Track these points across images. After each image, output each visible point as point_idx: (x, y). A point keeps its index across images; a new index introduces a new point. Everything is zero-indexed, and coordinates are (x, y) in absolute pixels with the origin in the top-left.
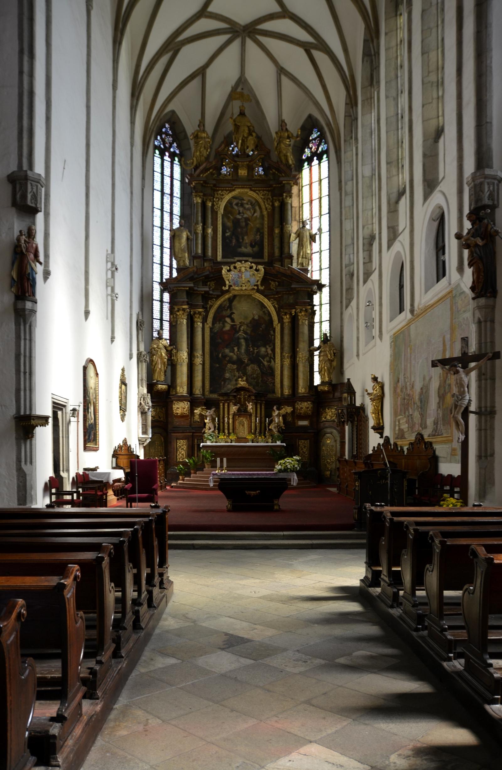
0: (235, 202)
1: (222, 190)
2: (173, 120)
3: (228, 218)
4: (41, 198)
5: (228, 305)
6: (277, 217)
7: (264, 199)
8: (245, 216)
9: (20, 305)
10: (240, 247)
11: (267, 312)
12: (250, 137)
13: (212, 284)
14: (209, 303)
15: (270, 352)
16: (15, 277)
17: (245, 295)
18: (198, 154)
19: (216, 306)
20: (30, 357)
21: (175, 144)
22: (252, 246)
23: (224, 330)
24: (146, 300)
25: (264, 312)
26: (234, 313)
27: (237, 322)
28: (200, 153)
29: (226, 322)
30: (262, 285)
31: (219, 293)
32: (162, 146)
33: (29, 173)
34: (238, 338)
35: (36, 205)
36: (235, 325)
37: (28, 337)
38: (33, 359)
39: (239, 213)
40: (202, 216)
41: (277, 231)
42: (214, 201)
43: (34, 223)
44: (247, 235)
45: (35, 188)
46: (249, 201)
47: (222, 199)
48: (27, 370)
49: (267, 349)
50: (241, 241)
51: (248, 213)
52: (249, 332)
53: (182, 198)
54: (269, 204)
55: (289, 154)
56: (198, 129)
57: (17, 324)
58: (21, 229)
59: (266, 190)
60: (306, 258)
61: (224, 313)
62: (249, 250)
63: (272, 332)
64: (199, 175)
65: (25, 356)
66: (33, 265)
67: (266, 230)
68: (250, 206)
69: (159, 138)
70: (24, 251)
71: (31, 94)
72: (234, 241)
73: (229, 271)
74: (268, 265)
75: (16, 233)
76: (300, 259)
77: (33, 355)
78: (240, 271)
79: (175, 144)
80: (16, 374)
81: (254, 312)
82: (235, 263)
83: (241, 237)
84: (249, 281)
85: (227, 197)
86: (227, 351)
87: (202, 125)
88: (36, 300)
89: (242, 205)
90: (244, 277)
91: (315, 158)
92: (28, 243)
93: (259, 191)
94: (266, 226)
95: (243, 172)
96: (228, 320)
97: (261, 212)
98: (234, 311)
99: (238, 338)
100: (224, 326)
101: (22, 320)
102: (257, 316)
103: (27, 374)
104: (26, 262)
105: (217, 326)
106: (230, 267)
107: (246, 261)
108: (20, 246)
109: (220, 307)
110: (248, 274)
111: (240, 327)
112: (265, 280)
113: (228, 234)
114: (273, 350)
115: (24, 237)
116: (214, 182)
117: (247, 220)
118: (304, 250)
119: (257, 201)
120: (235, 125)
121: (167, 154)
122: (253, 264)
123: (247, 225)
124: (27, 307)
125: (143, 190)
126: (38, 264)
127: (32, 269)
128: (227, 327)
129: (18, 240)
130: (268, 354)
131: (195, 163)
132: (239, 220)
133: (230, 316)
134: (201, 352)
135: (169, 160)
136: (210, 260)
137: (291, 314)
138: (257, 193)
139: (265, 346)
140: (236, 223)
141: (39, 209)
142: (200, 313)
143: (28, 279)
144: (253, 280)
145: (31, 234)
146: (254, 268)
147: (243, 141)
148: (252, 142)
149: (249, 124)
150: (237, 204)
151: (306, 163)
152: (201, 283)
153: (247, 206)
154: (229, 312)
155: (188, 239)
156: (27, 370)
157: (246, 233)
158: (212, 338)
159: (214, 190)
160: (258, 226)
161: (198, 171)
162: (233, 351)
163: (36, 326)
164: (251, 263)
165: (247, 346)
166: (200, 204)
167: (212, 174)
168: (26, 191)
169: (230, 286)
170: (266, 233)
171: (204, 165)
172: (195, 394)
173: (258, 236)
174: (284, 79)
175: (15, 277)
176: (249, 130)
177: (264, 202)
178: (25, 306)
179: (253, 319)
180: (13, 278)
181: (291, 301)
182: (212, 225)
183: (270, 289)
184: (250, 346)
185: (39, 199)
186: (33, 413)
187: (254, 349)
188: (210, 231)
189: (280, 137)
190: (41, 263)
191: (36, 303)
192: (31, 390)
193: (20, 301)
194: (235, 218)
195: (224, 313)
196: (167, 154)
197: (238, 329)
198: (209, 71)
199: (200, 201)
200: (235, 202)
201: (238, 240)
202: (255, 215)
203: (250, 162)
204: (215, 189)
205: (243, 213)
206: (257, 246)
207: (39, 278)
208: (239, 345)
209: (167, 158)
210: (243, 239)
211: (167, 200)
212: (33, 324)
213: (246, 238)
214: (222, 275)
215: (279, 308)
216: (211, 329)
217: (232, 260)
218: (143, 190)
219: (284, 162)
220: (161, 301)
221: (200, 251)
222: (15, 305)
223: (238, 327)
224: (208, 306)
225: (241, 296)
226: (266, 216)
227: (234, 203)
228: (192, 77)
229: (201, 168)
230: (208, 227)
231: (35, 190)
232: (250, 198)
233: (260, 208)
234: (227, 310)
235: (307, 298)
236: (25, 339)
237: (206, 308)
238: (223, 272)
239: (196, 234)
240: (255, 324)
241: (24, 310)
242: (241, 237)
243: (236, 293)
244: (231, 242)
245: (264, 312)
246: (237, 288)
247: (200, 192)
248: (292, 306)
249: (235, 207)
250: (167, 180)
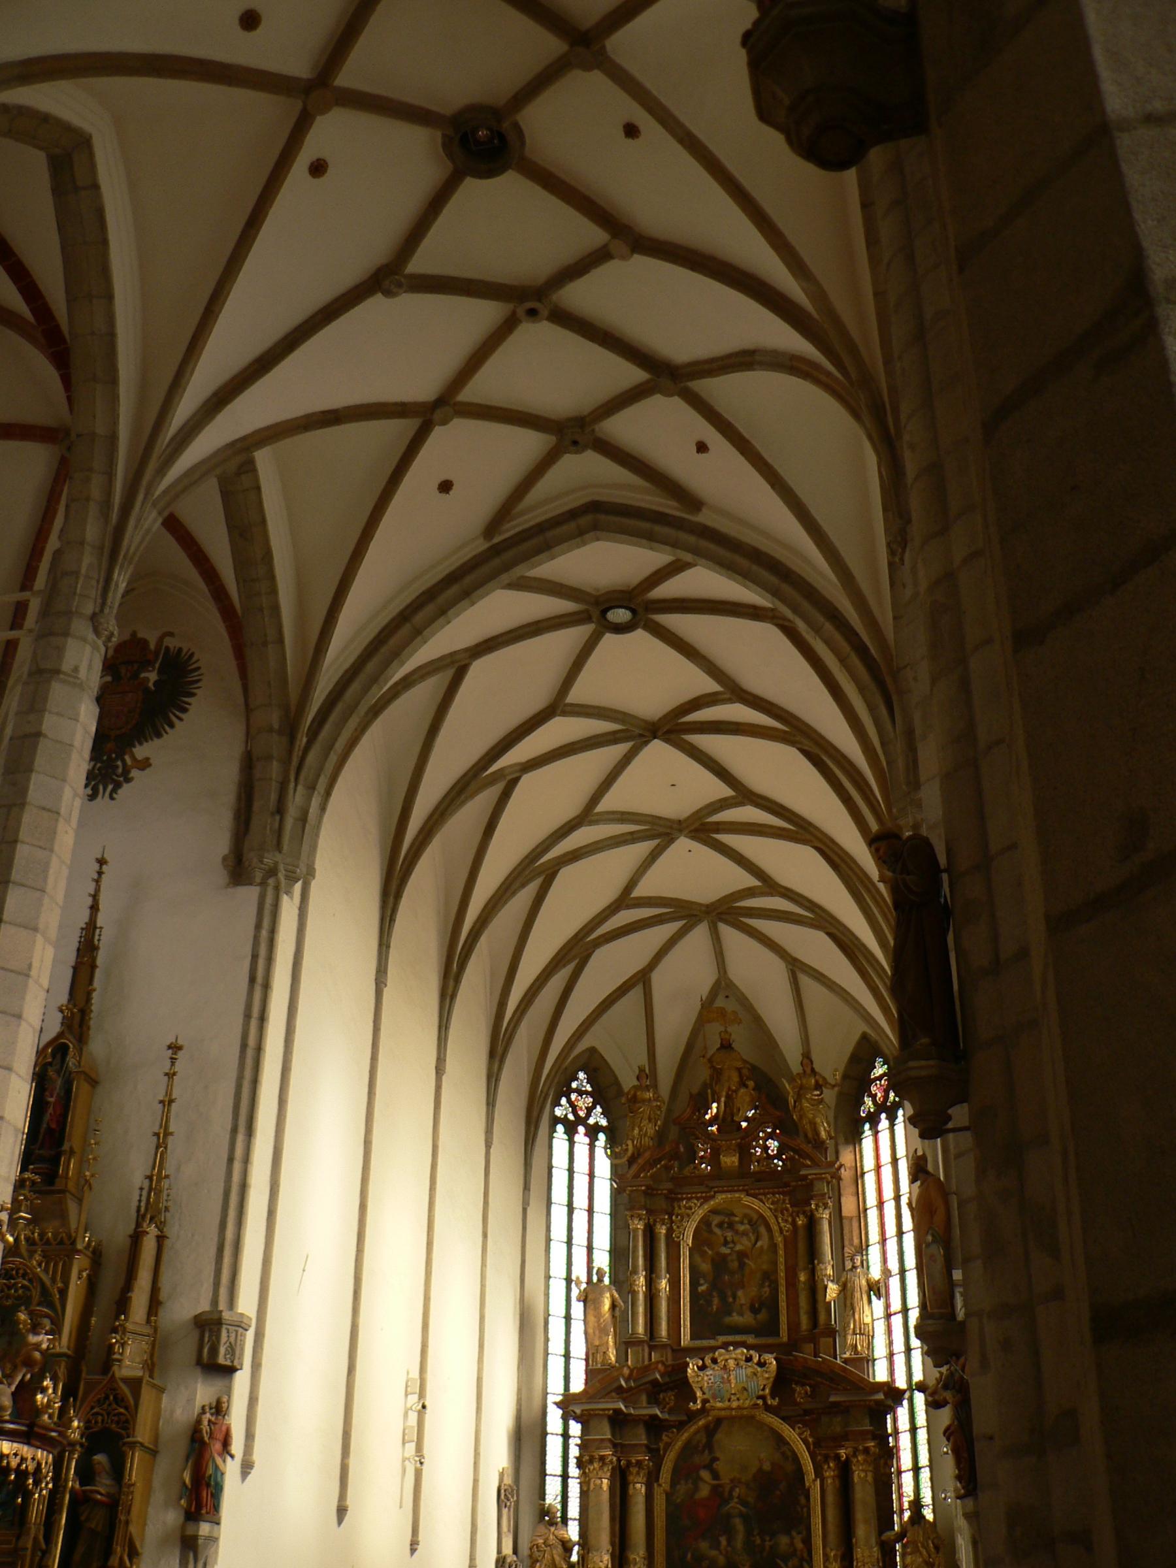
0: (716, 1220)
1: (689, 1199)
2: (594, 1065)
3: (703, 1254)
5: (704, 1441)
6: (802, 1246)
7: (776, 1210)
8: (738, 1247)
10: (729, 1314)
11: (789, 1454)
12: (743, 1090)
13: (670, 1397)
14: (664, 1437)
15: (799, 1545)
17: (741, 1417)
18: (636, 1131)
19: (679, 1444)
21: (599, 1109)
22: (754, 1310)
23: (697, 1496)
24: (527, 1438)
25: (783, 1454)
26: (716, 1459)
27: (725, 1480)
28: (641, 1130)
29: (702, 1479)
30: (773, 1398)
31: (685, 1418)
32: (571, 1117)
34: (729, 1516)
36: (719, 1486)
39: (726, 1243)
40: (645, 1256)
41: (802, 1277)
42: (672, 1222)
44: (743, 1287)
46: (745, 1216)
47: (689, 1216)
49: (792, 1538)
50: (731, 1300)
51: (745, 1240)
52: (751, 1500)
53: (614, 1215)
54: (786, 1221)
55: (818, 1120)
56: (636, 1083)
59: (779, 1193)
60: (860, 1334)
61: (697, 1459)
62: (747, 1319)
63: (803, 1501)
64: (636, 1176)
67: (782, 1274)
68: (748, 1227)
69: (564, 1101)
72: (716, 1301)
73: (702, 1368)
74: (784, 1352)
76: (849, 1337)
78: (725, 1367)
79: (599, 1109)
81: (762, 1455)
82: (713, 1349)
83: (729, 1293)
84: (745, 1389)
85: (700, 1213)
86: (704, 1545)
89: (731, 1226)
90: (733, 1381)
91: (883, 1116)
93: (765, 1194)
94: (782, 1267)
95: (730, 1160)
96: (705, 1474)
97: (771, 1237)
98: (718, 1455)
99: (729, 1516)
100: (696, 1489)
102: (768, 1464)
105: (683, 1488)
106: (703, 1360)
107: (737, 1345)
109: (687, 1445)
110: (743, 1373)
111: (732, 1490)
112: (782, 1383)
113: (702, 1288)
114: (807, 1542)
116: (670, 1185)
117: (742, 1255)
118: (857, 1317)
119: (761, 1216)
120: (713, 1067)
121: (581, 1129)
122: (752, 1352)
123: (742, 1265)
125: (525, 1211)
128: (704, 1492)
130: (795, 1550)
131: (630, 1153)
132: (725, 1256)
133: (709, 1467)
134: (642, 1551)
135: (587, 1140)
136: (664, 1346)
137: (838, 1457)
138: (761, 1200)
139: (788, 1533)
140: (720, 1263)
142: (639, 1464)
144: (755, 1386)
146: (756, 1359)
147: (728, 1097)
148: (747, 1099)
149: (739, 1064)
150: (720, 1225)
151: (867, 1126)
152: (644, 1398)
153: (741, 1228)
154: (706, 1457)
155: (613, 1306)
157: (742, 1285)
159: (673, 1200)
160: (765, 1267)
161: (635, 1168)
162: (716, 1545)
164: (749, 1347)
165: (749, 1533)
166: (640, 1233)
167: (668, 1168)
169: (705, 1401)
170: (782, 1282)
171: (647, 1155)
173: (767, 1289)
174: (804, 980)
176: (741, 1076)
177: (776, 1218)
179: (760, 1470)
181: (838, 1429)
182: (668, 1271)
183: (796, 1404)
184: (756, 1532)
187: (763, 1541)
188: (664, 1284)
189: (801, 1087)
194: (718, 1254)
195: (697, 1459)
196: (581, 1129)
197: (726, 1494)
199: (640, 1226)
200: (716, 1220)
201: (723, 1299)
202: (759, 1244)
203: (742, 1139)
204: (672, 1198)
205: (733, 1242)
206: (764, 1310)
208: (730, 1532)
209: (581, 1137)
210: (735, 1297)
211: (580, 1218)
213: (740, 1293)
215: (814, 1443)
216: (668, 1495)
217: (712, 1343)
218: (525, 1211)
219: (810, 1135)
220: (566, 1436)
221: (641, 1329)
223: (727, 1489)
224: (661, 1445)
225: (732, 1418)
226: (781, 1246)
227: (715, 1223)
228: (622, 991)
229: (641, 1161)
230: (659, 1277)
232: (747, 1211)
233: (769, 1230)
234: (703, 1451)
235: (867, 1421)
237: (658, 1450)
238: (691, 1370)
239: (634, 1293)
240: (764, 1482)
242: (729, 1293)
243: (723, 1413)
244: (709, 1303)
245: (783, 1454)
246: (719, 1405)
247: (639, 1209)
248: (839, 1440)
249: (717, 1231)
250: (581, 1182)
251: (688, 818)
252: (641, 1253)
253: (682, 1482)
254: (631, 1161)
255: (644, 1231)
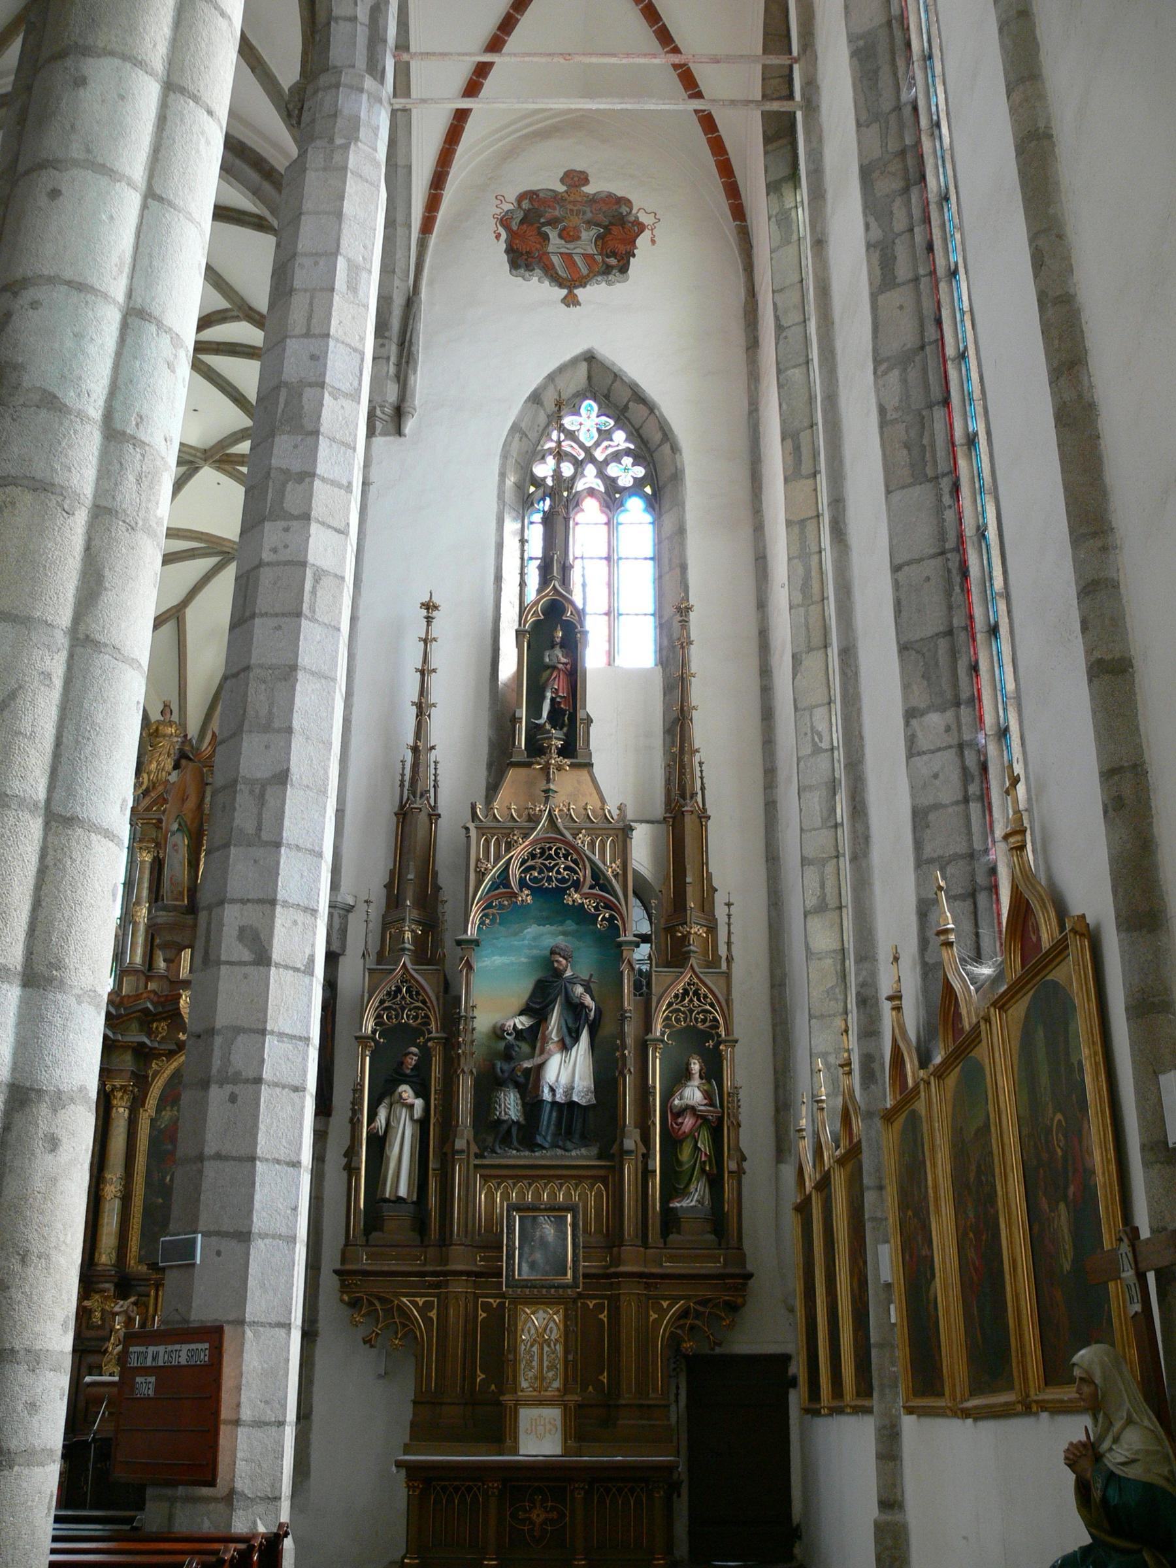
13: (162, 1027)
19: (168, 1073)
31: (174, 1047)
40: (150, 888)
64: (148, 809)
87: (168, 710)
105: (167, 1114)
131: (144, 787)
136: (161, 977)
158: (154, 1142)
166: (148, 866)
172: (97, 1265)
198: (190, 612)
214: (179, 1008)
224: (150, 1073)
251: (213, 447)
252: (146, 885)
253: (168, 1108)
254: (146, 793)
255: (152, 864)
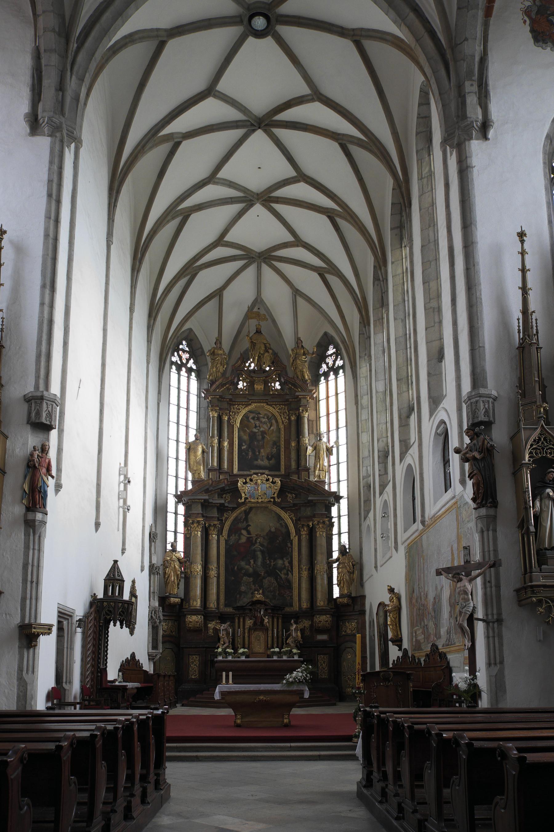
4: (55, 417)
9: (30, 516)
16: (26, 489)
20: (38, 566)
33: (45, 394)
35: (51, 422)
37: (36, 547)
38: (41, 568)
43: (48, 440)
45: (51, 406)
48: (35, 579)
57: (27, 535)
58: (34, 445)
65: (33, 566)
66: (45, 479)
70: (37, 465)
71: (51, 322)
75: (30, 448)
77: (41, 565)
80: (23, 583)
88: (47, 511)
92: (42, 458)
101: (31, 531)
103: (34, 584)
104: (38, 475)
108: (34, 460)
115: (37, 452)
124: (37, 518)
126: (49, 477)
127: (44, 482)
129: (32, 455)
141: (54, 426)
143: (40, 492)
145: (44, 449)
156: (35, 579)
163: (45, 537)
168: (42, 410)
175: (26, 489)
178: (35, 517)
180: (25, 490)
185: (53, 418)
186: (38, 622)
190: (53, 477)
191: (47, 514)
192: (37, 599)
193: (30, 513)
207: (51, 491)
212: (42, 535)
222: (25, 515)
231: (50, 409)
236: (34, 549)
241: (34, 521)
